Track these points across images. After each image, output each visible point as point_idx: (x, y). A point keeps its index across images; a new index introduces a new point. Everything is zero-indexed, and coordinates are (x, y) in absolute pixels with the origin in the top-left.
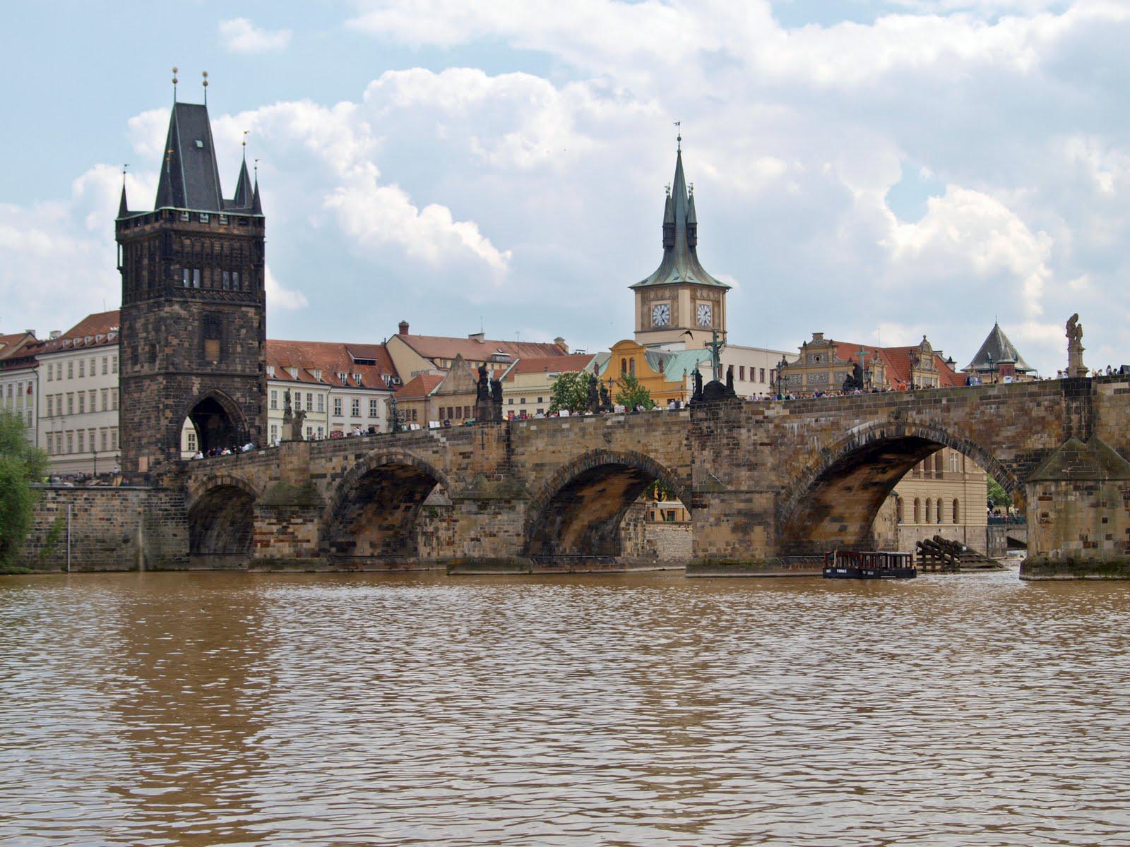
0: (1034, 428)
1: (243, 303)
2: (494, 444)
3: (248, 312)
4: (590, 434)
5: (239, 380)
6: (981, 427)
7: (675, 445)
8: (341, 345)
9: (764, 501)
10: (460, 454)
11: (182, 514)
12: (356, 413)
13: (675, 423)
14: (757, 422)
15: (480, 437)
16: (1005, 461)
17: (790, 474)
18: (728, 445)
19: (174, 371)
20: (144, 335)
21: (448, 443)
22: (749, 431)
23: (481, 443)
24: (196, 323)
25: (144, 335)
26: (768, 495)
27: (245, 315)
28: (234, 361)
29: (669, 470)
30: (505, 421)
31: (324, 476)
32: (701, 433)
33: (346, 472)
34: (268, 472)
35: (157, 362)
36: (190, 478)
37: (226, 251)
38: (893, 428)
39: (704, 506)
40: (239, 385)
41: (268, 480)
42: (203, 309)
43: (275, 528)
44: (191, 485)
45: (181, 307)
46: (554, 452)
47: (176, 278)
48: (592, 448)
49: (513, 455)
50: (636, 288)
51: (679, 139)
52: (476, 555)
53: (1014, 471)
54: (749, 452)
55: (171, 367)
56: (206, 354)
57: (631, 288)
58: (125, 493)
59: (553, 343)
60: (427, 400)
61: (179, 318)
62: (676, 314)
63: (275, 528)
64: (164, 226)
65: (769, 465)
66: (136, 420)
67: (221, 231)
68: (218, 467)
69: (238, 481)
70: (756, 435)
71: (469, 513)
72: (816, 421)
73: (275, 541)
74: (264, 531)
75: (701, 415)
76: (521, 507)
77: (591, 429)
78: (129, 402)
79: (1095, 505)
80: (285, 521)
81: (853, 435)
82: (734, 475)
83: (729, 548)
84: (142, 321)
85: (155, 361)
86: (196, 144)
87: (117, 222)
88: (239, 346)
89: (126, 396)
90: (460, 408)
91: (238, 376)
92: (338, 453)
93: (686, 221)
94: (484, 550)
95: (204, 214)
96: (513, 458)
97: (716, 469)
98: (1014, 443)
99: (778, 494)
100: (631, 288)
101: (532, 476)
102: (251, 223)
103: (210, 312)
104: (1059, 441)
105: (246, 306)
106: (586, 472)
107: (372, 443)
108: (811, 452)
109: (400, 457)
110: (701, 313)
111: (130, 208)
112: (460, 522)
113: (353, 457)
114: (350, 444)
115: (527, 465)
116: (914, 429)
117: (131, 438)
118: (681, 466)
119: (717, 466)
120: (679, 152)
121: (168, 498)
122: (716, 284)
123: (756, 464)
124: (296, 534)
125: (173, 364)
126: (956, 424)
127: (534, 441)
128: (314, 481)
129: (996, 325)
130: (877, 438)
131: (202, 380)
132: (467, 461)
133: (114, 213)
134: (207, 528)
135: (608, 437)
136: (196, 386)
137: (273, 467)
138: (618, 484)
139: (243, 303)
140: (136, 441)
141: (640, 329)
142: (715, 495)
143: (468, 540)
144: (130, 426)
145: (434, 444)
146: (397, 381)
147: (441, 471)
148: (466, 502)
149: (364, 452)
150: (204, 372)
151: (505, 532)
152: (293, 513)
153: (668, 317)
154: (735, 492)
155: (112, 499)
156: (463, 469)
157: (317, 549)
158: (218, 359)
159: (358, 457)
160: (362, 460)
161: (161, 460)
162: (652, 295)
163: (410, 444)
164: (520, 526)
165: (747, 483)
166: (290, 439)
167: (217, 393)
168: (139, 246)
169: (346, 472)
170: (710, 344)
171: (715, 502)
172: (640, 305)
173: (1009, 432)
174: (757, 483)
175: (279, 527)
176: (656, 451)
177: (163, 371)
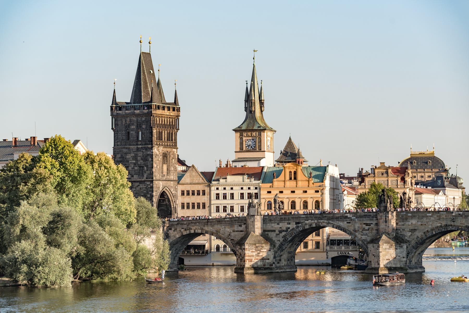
4: (443, 218)
5: (172, 183)
10: (364, 224)
15: (384, 218)
20: (134, 161)
24: (161, 157)
25: (134, 161)
28: (171, 174)
31: (274, 231)
35: (145, 175)
36: (171, 229)
37: (168, 123)
40: (172, 185)
41: (232, 231)
42: (163, 150)
43: (254, 254)
48: (444, 223)
50: (235, 130)
57: (233, 130)
61: (156, 155)
63: (254, 254)
67: (168, 114)
68: (193, 225)
71: (386, 249)
73: (254, 259)
74: (250, 255)
76: (405, 247)
80: (259, 250)
84: (133, 155)
88: (172, 167)
90: (184, 191)
91: (171, 181)
92: (283, 221)
94: (391, 264)
100: (233, 130)
107: (306, 218)
109: (326, 224)
113: (294, 223)
114: (292, 218)
115: (406, 230)
125: (155, 176)
128: (266, 233)
129: (290, 137)
131: (163, 183)
132: (368, 227)
137: (235, 226)
141: (238, 150)
143: (385, 260)
145: (348, 219)
149: (302, 221)
151: (399, 256)
153: (254, 145)
156: (366, 230)
157: (272, 262)
158: (166, 173)
159: (297, 223)
160: (300, 225)
163: (332, 219)
164: (404, 254)
167: (166, 189)
168: (128, 119)
169: (289, 230)
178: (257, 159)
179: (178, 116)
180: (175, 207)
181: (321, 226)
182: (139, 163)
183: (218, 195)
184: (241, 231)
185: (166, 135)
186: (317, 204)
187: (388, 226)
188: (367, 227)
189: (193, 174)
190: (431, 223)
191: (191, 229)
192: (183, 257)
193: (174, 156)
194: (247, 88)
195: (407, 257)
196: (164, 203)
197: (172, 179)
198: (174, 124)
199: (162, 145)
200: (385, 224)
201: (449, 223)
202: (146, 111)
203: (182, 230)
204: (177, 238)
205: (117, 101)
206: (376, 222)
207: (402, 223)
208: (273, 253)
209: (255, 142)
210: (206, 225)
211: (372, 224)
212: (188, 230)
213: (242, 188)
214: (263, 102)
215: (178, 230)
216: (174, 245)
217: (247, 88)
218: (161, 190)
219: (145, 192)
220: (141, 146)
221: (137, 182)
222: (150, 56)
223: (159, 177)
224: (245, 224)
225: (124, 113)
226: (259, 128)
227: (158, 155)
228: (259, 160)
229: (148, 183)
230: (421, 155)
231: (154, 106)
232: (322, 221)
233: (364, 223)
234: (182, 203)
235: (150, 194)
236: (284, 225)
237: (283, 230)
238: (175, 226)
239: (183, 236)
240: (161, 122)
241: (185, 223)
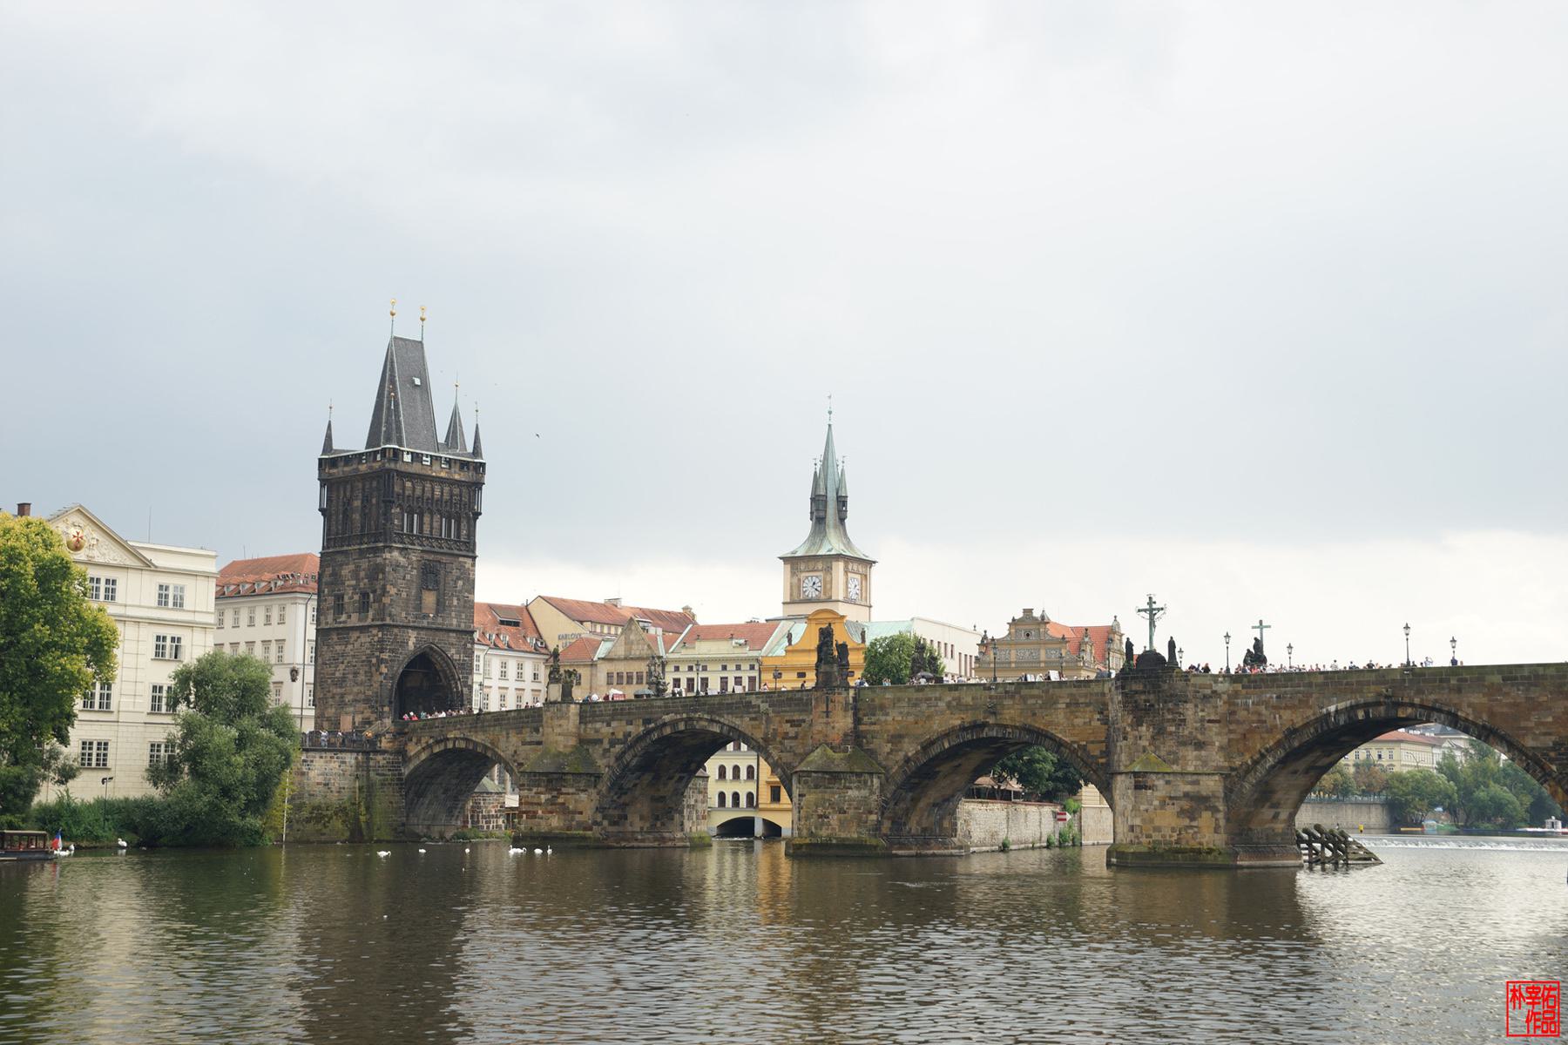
1: (461, 553)
3: (465, 563)
5: (454, 635)
8: (485, 604)
9: (1212, 783)
11: (399, 779)
12: (504, 675)
14: (1205, 696)
18: (1174, 720)
19: (391, 623)
20: (354, 582)
22: (1196, 706)
23: (825, 710)
24: (415, 572)
25: (354, 582)
26: (1217, 778)
27: (462, 565)
29: (1076, 746)
30: (853, 687)
31: (600, 741)
32: (1136, 707)
33: (629, 739)
35: (371, 614)
37: (446, 497)
39: (1146, 788)
40: (453, 640)
43: (543, 798)
44: (412, 749)
45: (400, 553)
47: (396, 522)
49: (861, 724)
50: (785, 559)
54: (1196, 729)
55: (388, 618)
56: (423, 605)
57: (781, 558)
58: (343, 755)
59: (681, 611)
60: (593, 665)
62: (828, 586)
63: (543, 798)
64: (387, 465)
65: (1217, 744)
66: (337, 674)
67: (443, 474)
69: (476, 744)
70: (1203, 711)
72: (1278, 697)
78: (328, 656)
81: (1329, 714)
82: (1181, 754)
83: (1175, 834)
84: (352, 567)
85: (368, 612)
86: (413, 382)
87: (320, 460)
88: (455, 599)
91: (454, 631)
93: (837, 493)
95: (427, 456)
96: (862, 728)
100: (781, 558)
101: (888, 748)
102: (471, 468)
103: (428, 560)
105: (464, 556)
106: (959, 745)
107: (665, 707)
110: (851, 585)
112: (807, 796)
113: (641, 721)
117: (329, 695)
118: (1093, 742)
119: (1157, 743)
121: (385, 762)
123: (1204, 743)
124: (567, 805)
125: (390, 615)
130: (1360, 718)
131: (418, 634)
132: (796, 729)
133: (318, 453)
134: (420, 795)
136: (412, 640)
138: (976, 758)
139: (461, 553)
140: (337, 697)
141: (788, 600)
142: (1160, 776)
144: (329, 681)
146: (542, 643)
147: (761, 741)
150: (420, 625)
154: (1182, 774)
155: (331, 761)
158: (434, 612)
159: (646, 722)
160: (653, 725)
161: (372, 719)
163: (719, 709)
165: (1194, 763)
166: (560, 700)
167: (431, 648)
168: (349, 487)
169: (629, 739)
170: (1145, 610)
171: (1160, 783)
172: (789, 576)
174: (1205, 763)
177: (379, 623)
179: (478, 485)
180: (462, 691)
181: (697, 727)
182: (362, 585)
188: (792, 731)
191: (448, 739)
193: (462, 574)
194: (816, 472)
195: (883, 813)
197: (454, 627)
203: (431, 741)
205: (335, 447)
210: (473, 730)
211: (804, 721)
212: (441, 741)
213: (724, 668)
214: (843, 499)
215: (423, 740)
217: (816, 472)
219: (368, 652)
221: (356, 630)
222: (423, 348)
223: (406, 618)
225: (341, 475)
226: (829, 553)
227: (402, 567)
231: (392, 450)
233: (787, 718)
236: (620, 728)
237: (618, 740)
238: (419, 731)
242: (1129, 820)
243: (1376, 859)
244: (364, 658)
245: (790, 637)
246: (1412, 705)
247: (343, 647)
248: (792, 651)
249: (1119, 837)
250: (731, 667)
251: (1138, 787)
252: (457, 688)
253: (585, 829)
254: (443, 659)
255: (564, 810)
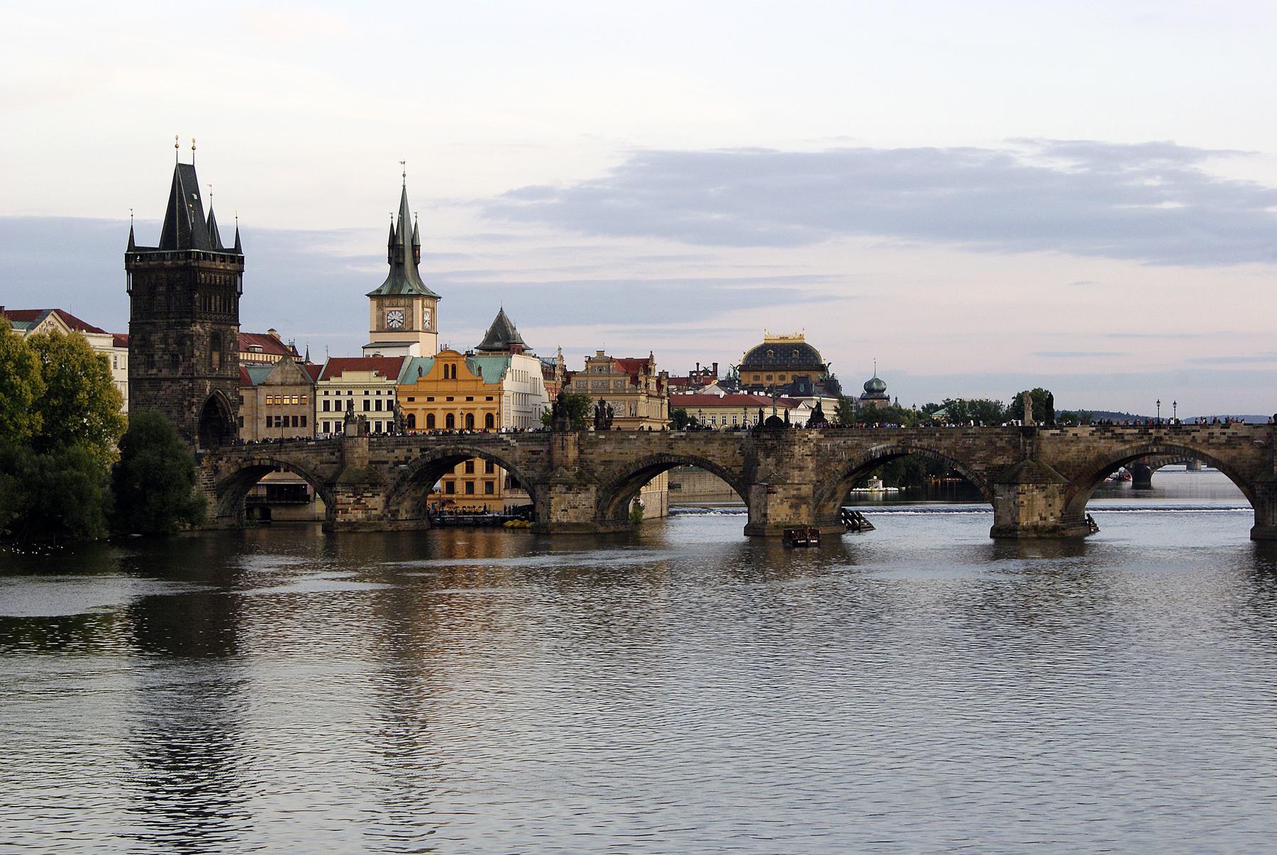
0: (998, 453)
2: (572, 446)
4: (655, 442)
5: (228, 382)
6: (963, 451)
7: (730, 453)
10: (530, 451)
13: (729, 439)
14: (804, 442)
15: (561, 442)
16: (979, 470)
17: (824, 473)
21: (517, 444)
22: (800, 447)
31: (387, 462)
33: (410, 461)
34: (319, 458)
35: (181, 369)
36: (221, 459)
37: (223, 283)
38: (900, 449)
39: (775, 493)
40: (229, 386)
43: (352, 500)
46: (621, 453)
48: (656, 452)
51: (404, 175)
52: (565, 520)
53: (985, 476)
57: (367, 295)
59: (267, 333)
61: (199, 335)
63: (352, 500)
64: (193, 264)
67: (221, 267)
68: (257, 452)
70: (803, 450)
71: (561, 492)
72: (845, 442)
74: (343, 502)
75: (766, 436)
76: (593, 489)
77: (656, 440)
79: (1046, 497)
82: (791, 474)
86: (193, 197)
89: (138, 393)
91: (228, 379)
93: (412, 243)
96: (582, 456)
97: (777, 470)
98: (984, 460)
99: (815, 485)
100: (367, 295)
104: (1014, 460)
107: (438, 441)
108: (840, 461)
109: (466, 451)
111: (137, 244)
113: (419, 449)
116: (914, 450)
119: (778, 468)
120: (404, 186)
122: (434, 295)
124: (367, 504)
126: (945, 448)
127: (602, 446)
128: (374, 466)
131: (211, 383)
135: (670, 446)
137: (324, 454)
141: (375, 330)
145: (504, 444)
148: (558, 485)
149: (430, 446)
152: (365, 489)
156: (533, 462)
159: (422, 450)
162: (387, 302)
168: (154, 276)
173: (982, 454)
175: (354, 499)
176: (714, 456)
178: (406, 344)
181: (462, 454)
182: (171, 348)
183: (326, 404)
184: (334, 463)
185: (218, 303)
186: (489, 419)
187: (565, 454)
189: (286, 368)
190: (635, 451)
191: (254, 459)
192: (269, 508)
194: (392, 225)
196: (217, 416)
197: (229, 376)
198: (232, 284)
199: (211, 320)
200: (561, 451)
201: (664, 451)
202: (181, 263)
203: (240, 460)
204: (232, 474)
206: (547, 448)
207: (590, 451)
208: (384, 499)
209: (403, 315)
211: (542, 451)
212: (249, 460)
213: (367, 393)
216: (229, 485)
218: (208, 393)
220: (173, 320)
224: (339, 451)
225: (147, 266)
226: (410, 293)
227: (202, 336)
228: (406, 345)
229: (185, 382)
230: (782, 341)
232: (461, 446)
234: (267, 417)
235: (189, 400)
237: (401, 462)
239: (241, 472)
240: (208, 281)
241: (244, 449)
242: (762, 510)
243: (873, 527)
244: (176, 401)
245: (420, 369)
246: (916, 447)
247: (156, 393)
248: (423, 381)
249: (753, 520)
250: (373, 392)
251: (769, 492)
252: (232, 420)
253: (379, 519)
254: (224, 400)
255: (366, 509)
